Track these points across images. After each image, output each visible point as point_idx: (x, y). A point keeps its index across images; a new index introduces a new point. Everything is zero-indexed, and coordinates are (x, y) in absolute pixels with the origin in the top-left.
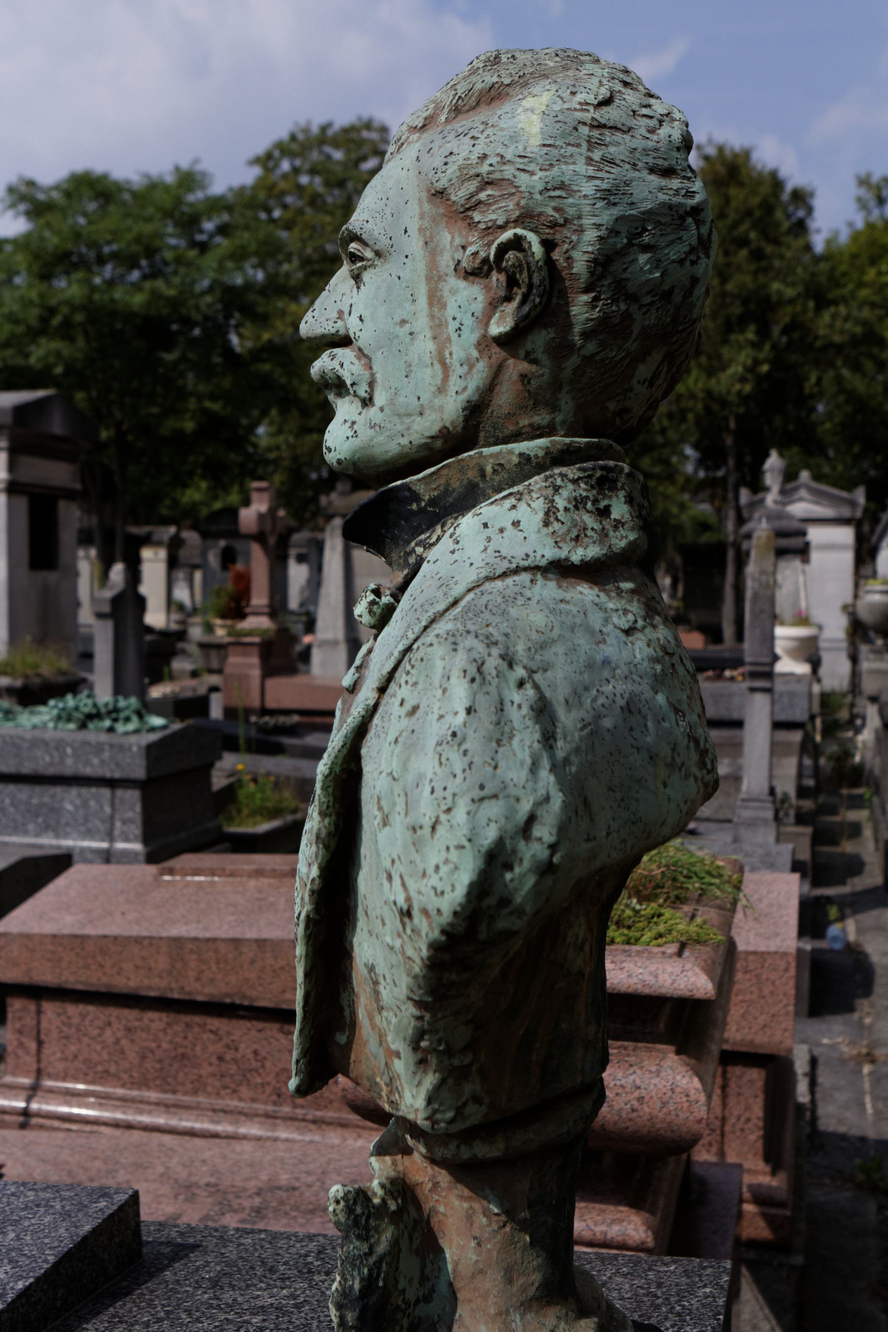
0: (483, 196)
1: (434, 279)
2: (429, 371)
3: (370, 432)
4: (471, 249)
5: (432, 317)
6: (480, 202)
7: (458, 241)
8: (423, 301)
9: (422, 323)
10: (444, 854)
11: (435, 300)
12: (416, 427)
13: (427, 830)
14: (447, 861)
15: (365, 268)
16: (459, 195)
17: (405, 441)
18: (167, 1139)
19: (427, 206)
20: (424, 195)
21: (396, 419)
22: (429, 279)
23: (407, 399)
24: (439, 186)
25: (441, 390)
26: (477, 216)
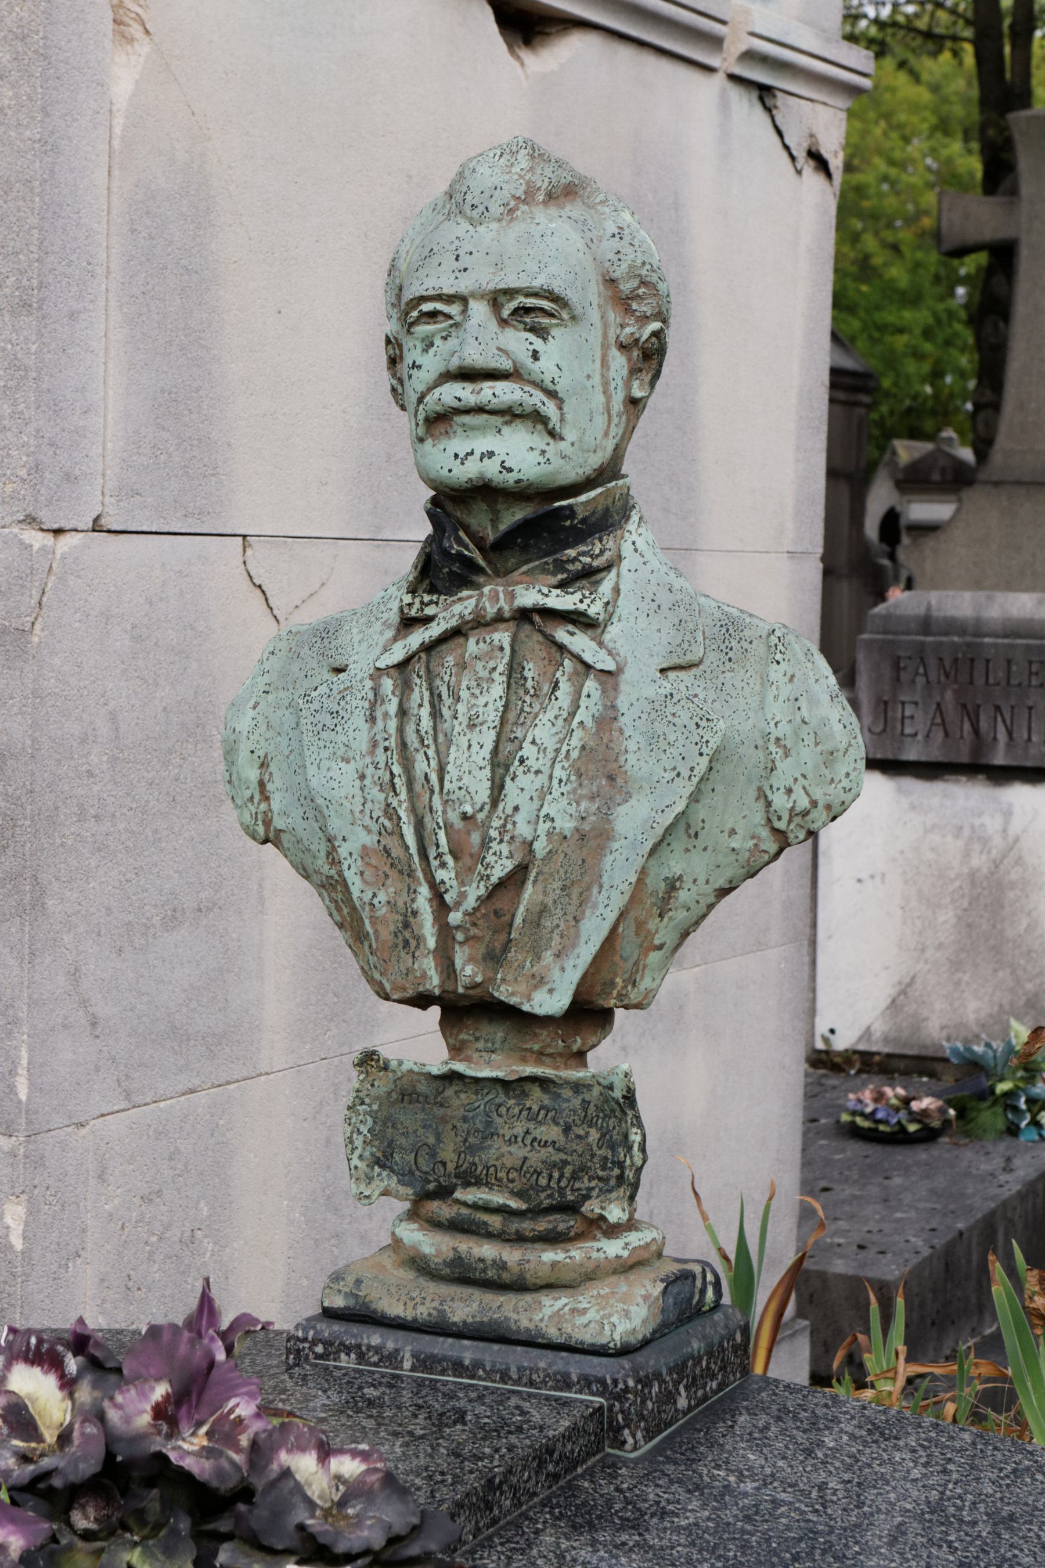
0: (641, 291)
1: (605, 347)
2: (601, 417)
3: (562, 462)
4: (628, 330)
5: (603, 376)
6: (638, 296)
7: (619, 320)
8: (598, 363)
9: (597, 379)
10: (853, 765)
11: (605, 364)
12: (590, 461)
13: (841, 753)
14: (855, 769)
15: (557, 325)
16: (626, 287)
17: (580, 471)
18: (116, 1108)
19: (602, 288)
20: (600, 278)
21: (580, 454)
22: (603, 346)
23: (589, 439)
24: (614, 276)
25: (606, 434)
26: (635, 306)
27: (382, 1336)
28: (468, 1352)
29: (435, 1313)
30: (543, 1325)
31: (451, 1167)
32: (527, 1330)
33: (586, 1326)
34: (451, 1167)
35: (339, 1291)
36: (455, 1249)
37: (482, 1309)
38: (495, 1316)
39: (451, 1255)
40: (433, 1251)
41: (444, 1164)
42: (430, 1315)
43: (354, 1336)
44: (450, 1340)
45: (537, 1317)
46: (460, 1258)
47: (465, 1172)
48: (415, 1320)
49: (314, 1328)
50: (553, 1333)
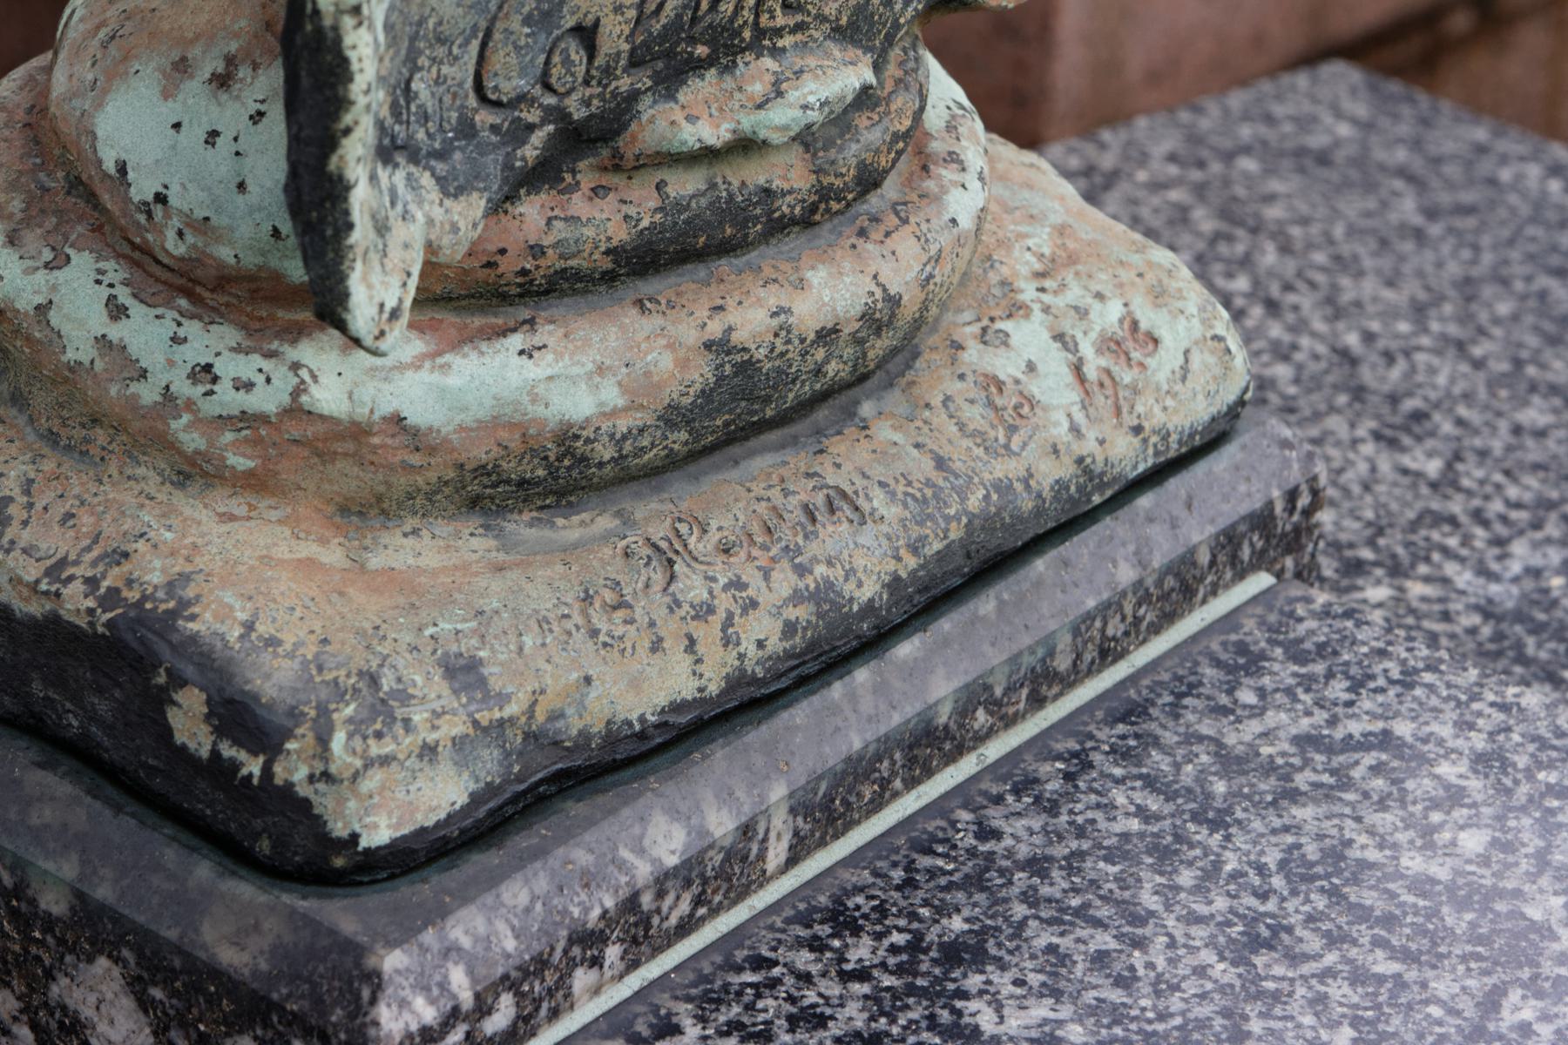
27: (675, 814)
28: (924, 674)
29: (802, 613)
30: (1089, 446)
31: (615, 37)
32: (1060, 486)
33: (1185, 369)
34: (615, 37)
35: (429, 751)
36: (718, 347)
37: (924, 503)
38: (974, 502)
39: (701, 372)
40: (611, 395)
41: (587, 35)
42: (790, 629)
43: (588, 880)
44: (862, 675)
45: (1061, 431)
46: (747, 367)
47: (675, 26)
48: (737, 681)
49: (450, 951)
50: (1125, 454)
